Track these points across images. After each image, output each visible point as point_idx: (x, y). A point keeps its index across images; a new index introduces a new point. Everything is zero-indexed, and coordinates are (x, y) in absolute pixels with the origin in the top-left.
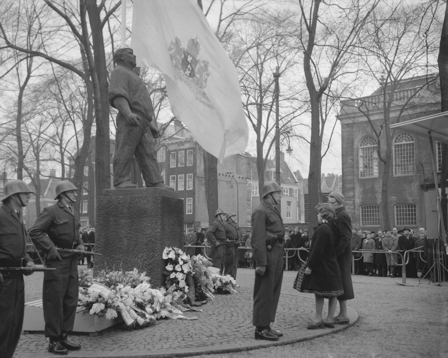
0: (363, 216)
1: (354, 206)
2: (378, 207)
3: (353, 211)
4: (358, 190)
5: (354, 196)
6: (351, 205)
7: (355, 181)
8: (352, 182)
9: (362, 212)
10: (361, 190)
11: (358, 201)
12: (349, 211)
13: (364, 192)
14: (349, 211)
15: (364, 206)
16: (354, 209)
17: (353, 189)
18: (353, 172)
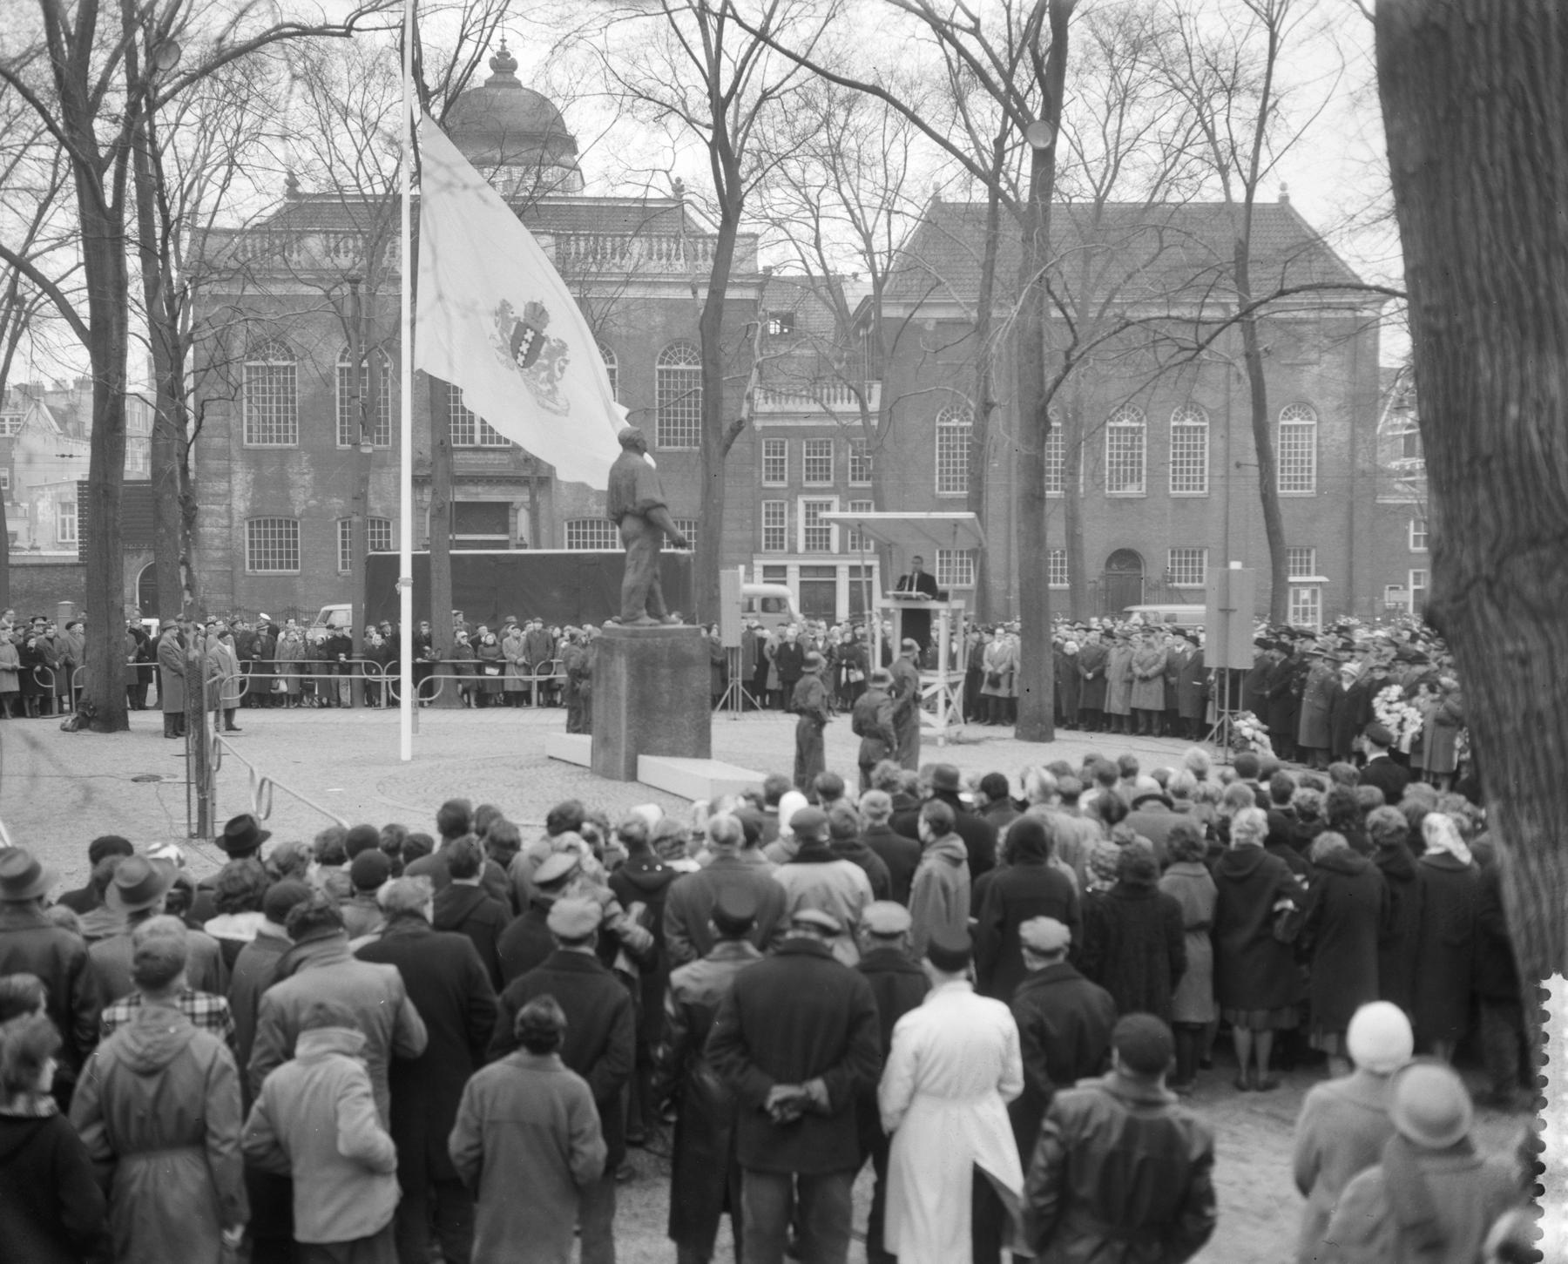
0: (252, 544)
1: (230, 517)
2: (295, 524)
3: (226, 531)
4: (240, 476)
5: (229, 492)
6: (220, 515)
7: (234, 453)
8: (225, 454)
9: (251, 535)
10: (250, 477)
11: (240, 505)
12: (215, 530)
13: (258, 483)
14: (215, 530)
15: (256, 520)
16: (230, 527)
17: (228, 474)
18: (228, 427)
